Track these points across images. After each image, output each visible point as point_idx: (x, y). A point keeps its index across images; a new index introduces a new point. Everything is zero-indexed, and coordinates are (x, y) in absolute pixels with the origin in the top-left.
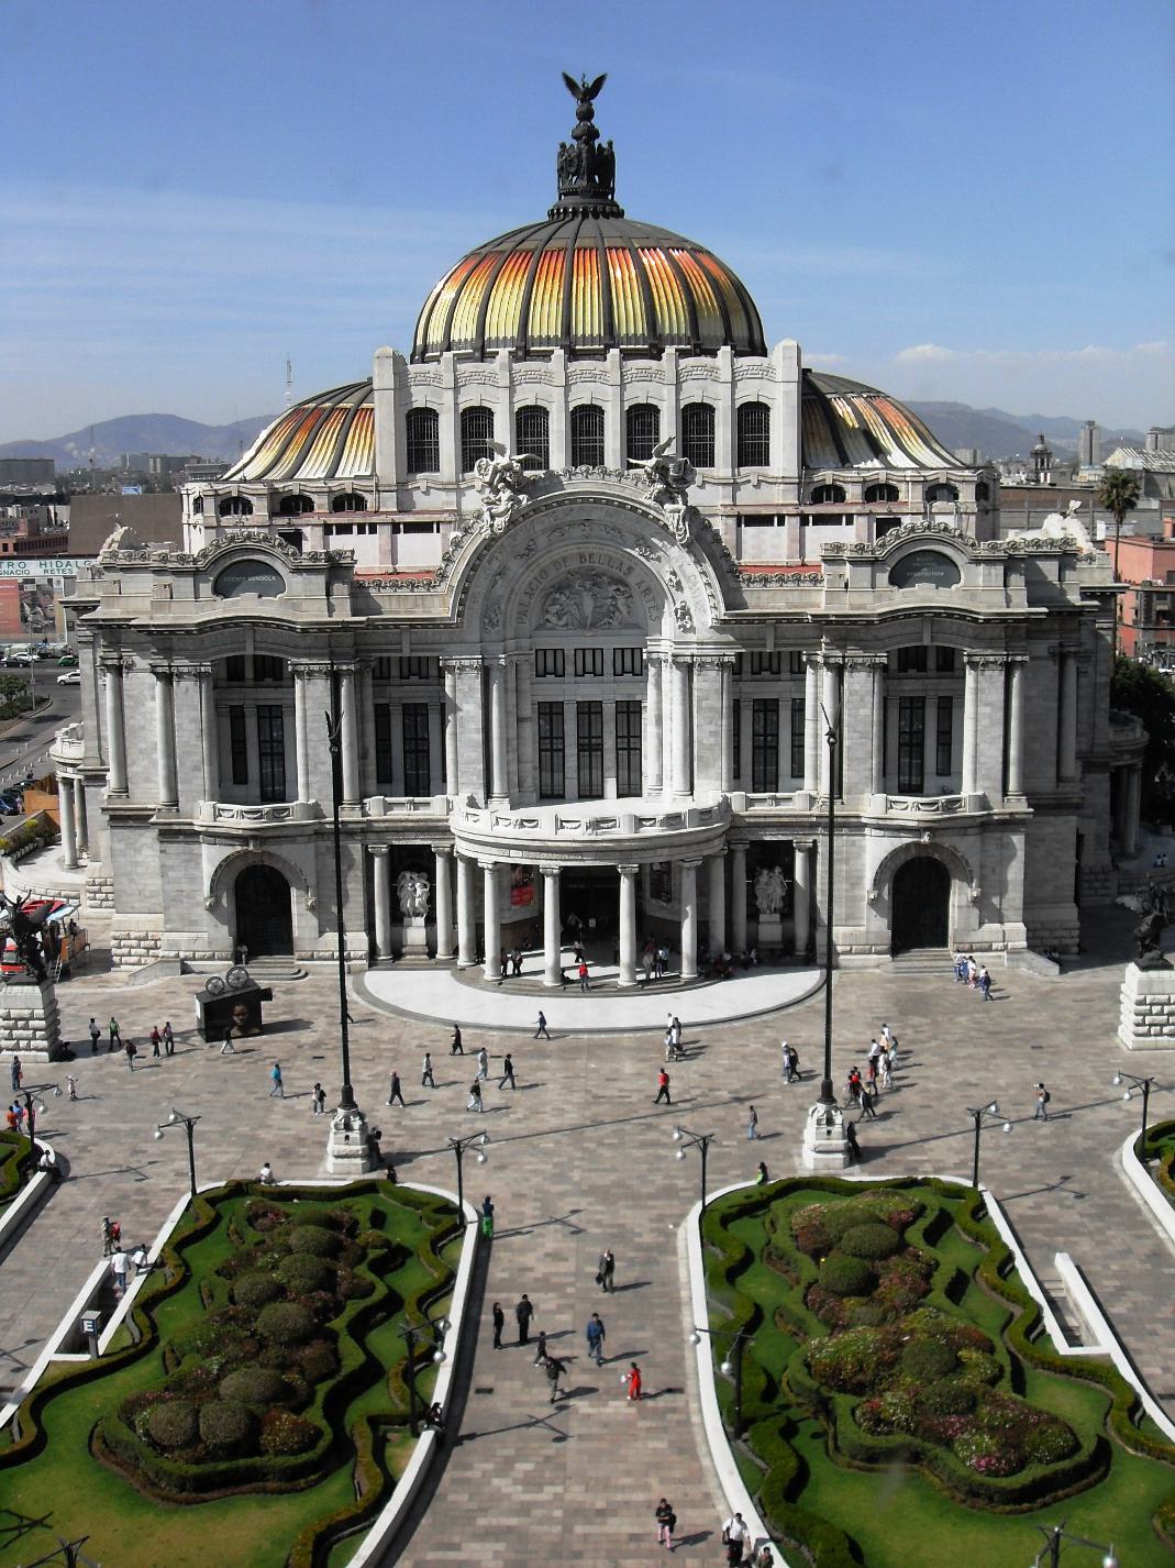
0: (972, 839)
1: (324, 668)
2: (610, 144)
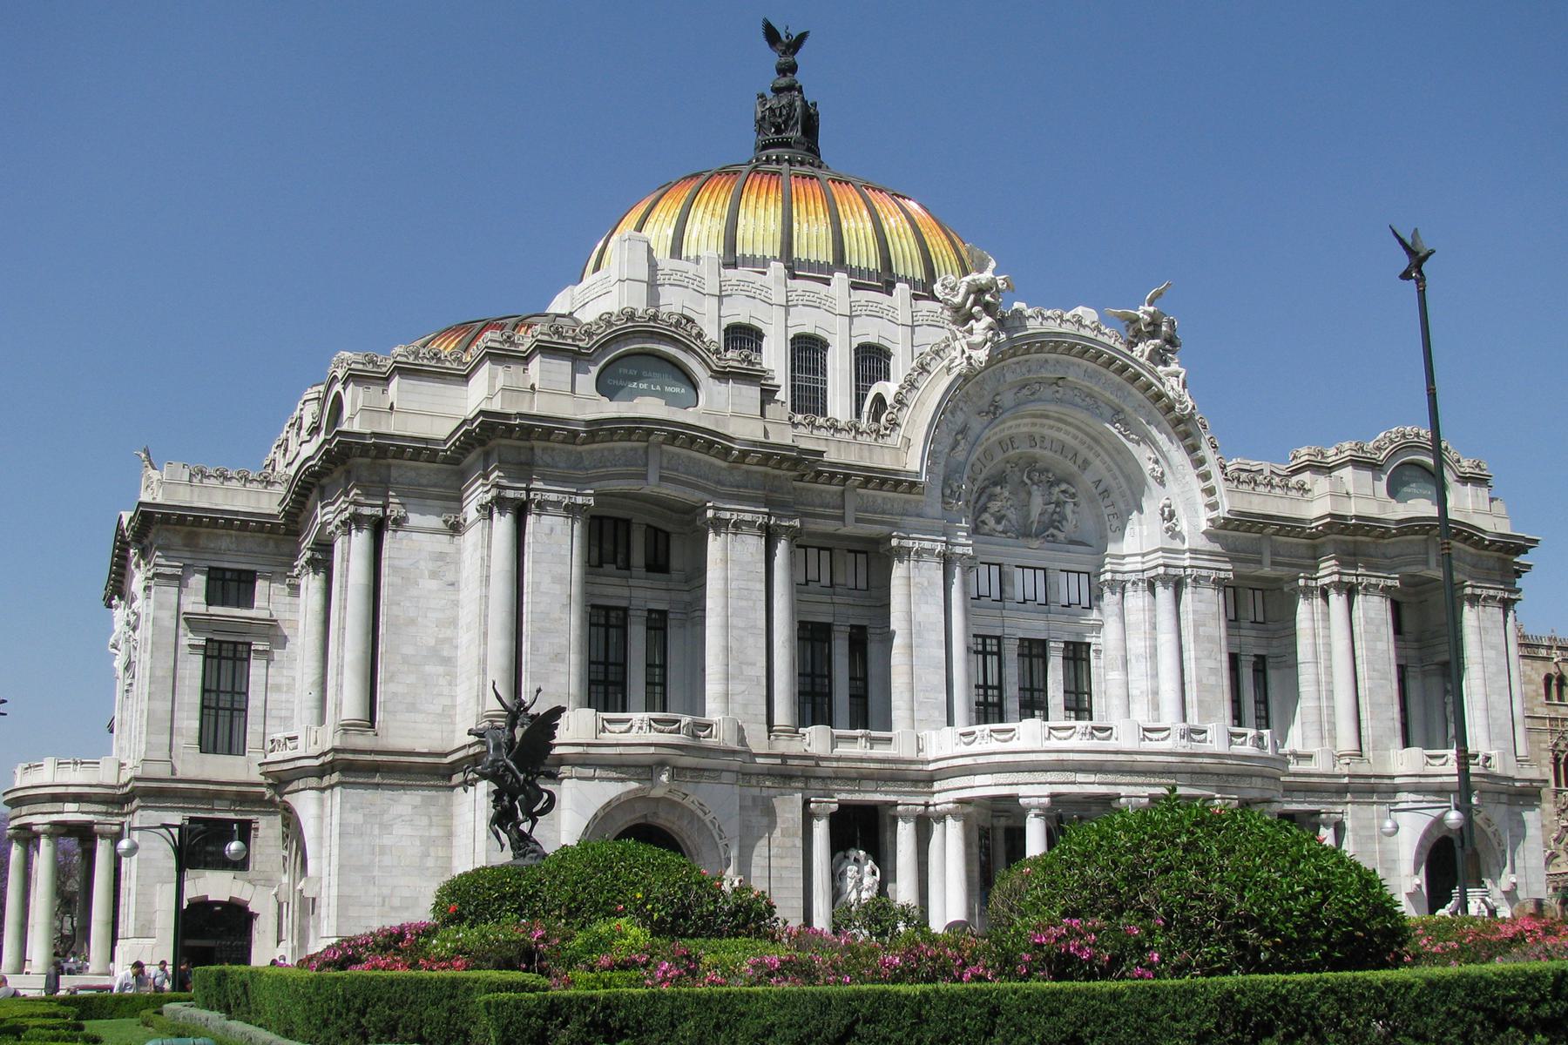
0: (1503, 808)
2: (815, 105)
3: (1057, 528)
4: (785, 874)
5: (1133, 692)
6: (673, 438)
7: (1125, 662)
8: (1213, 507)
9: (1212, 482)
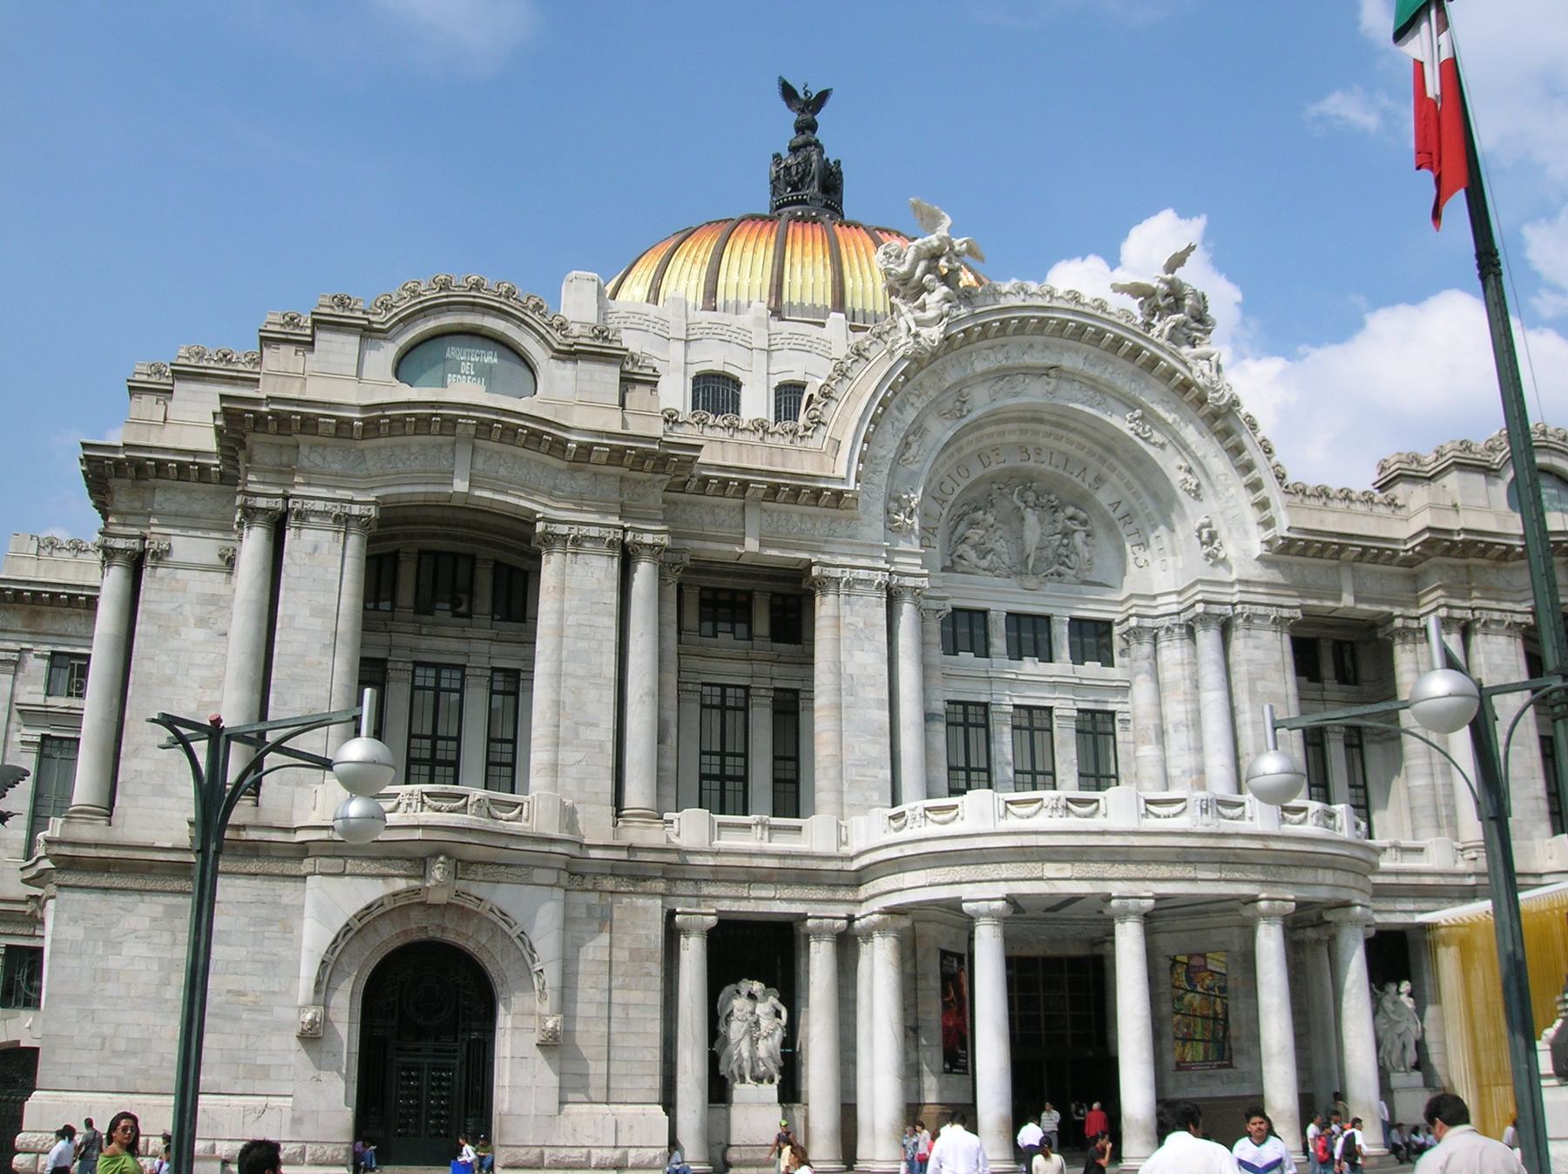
1: (611, 535)
2: (838, 163)
3: (1063, 564)
4: (633, 1013)
5: (1174, 772)
6: (484, 429)
7: (1161, 734)
8: (1268, 524)
9: (1264, 492)
